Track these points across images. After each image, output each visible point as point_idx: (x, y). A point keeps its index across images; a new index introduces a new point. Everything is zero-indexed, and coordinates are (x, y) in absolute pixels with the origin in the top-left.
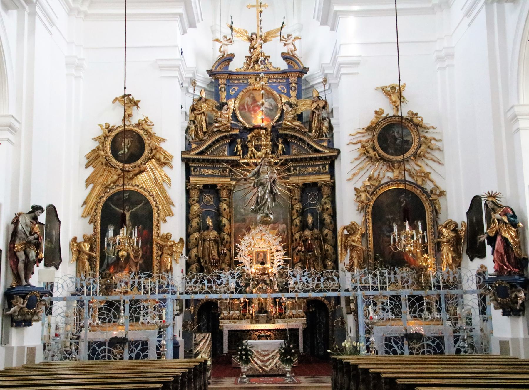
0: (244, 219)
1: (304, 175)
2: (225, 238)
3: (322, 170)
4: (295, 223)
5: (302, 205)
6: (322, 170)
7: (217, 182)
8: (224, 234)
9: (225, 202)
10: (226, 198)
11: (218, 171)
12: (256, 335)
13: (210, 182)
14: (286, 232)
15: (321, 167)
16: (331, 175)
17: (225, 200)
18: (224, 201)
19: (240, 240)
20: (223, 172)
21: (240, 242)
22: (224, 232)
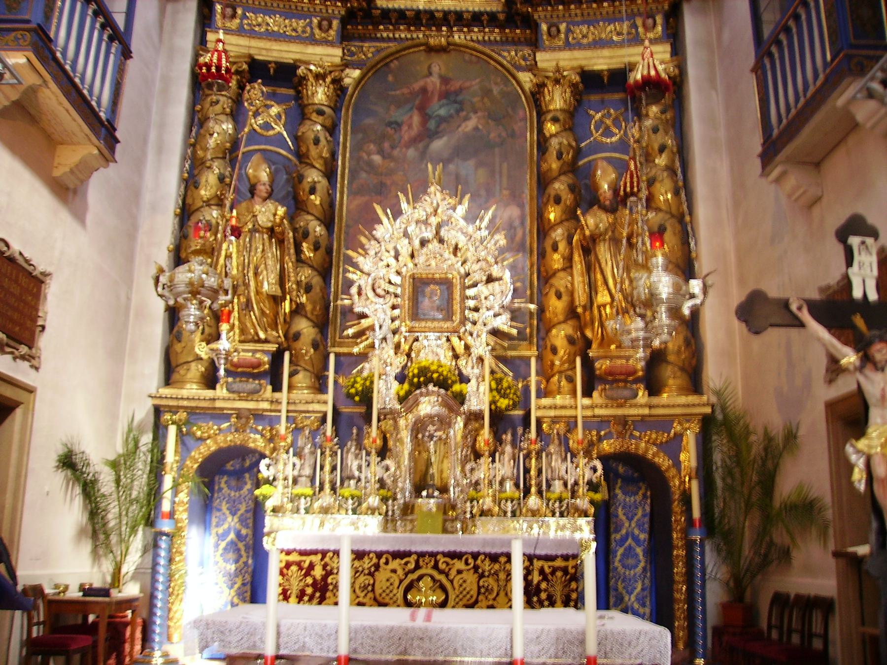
0: (382, 185)
1: (579, 46)
2: (311, 230)
3: (641, 30)
4: (553, 193)
5: (578, 141)
6: (641, 30)
7: (297, 57)
8: (310, 217)
9: (320, 119)
10: (325, 108)
11: (302, 23)
12: (394, 571)
13: (275, 54)
14: (519, 234)
15: (639, 22)
16: (671, 45)
17: (320, 113)
18: (314, 116)
19: (363, 240)
20: (320, 26)
21: (362, 246)
22: (308, 213)
